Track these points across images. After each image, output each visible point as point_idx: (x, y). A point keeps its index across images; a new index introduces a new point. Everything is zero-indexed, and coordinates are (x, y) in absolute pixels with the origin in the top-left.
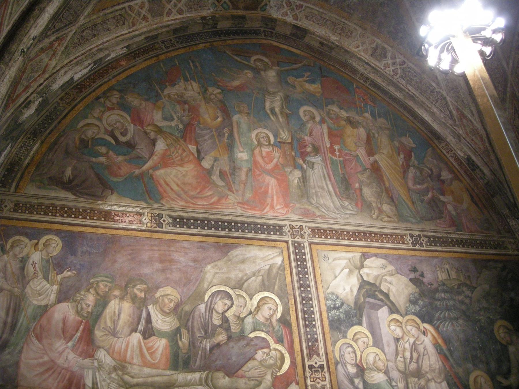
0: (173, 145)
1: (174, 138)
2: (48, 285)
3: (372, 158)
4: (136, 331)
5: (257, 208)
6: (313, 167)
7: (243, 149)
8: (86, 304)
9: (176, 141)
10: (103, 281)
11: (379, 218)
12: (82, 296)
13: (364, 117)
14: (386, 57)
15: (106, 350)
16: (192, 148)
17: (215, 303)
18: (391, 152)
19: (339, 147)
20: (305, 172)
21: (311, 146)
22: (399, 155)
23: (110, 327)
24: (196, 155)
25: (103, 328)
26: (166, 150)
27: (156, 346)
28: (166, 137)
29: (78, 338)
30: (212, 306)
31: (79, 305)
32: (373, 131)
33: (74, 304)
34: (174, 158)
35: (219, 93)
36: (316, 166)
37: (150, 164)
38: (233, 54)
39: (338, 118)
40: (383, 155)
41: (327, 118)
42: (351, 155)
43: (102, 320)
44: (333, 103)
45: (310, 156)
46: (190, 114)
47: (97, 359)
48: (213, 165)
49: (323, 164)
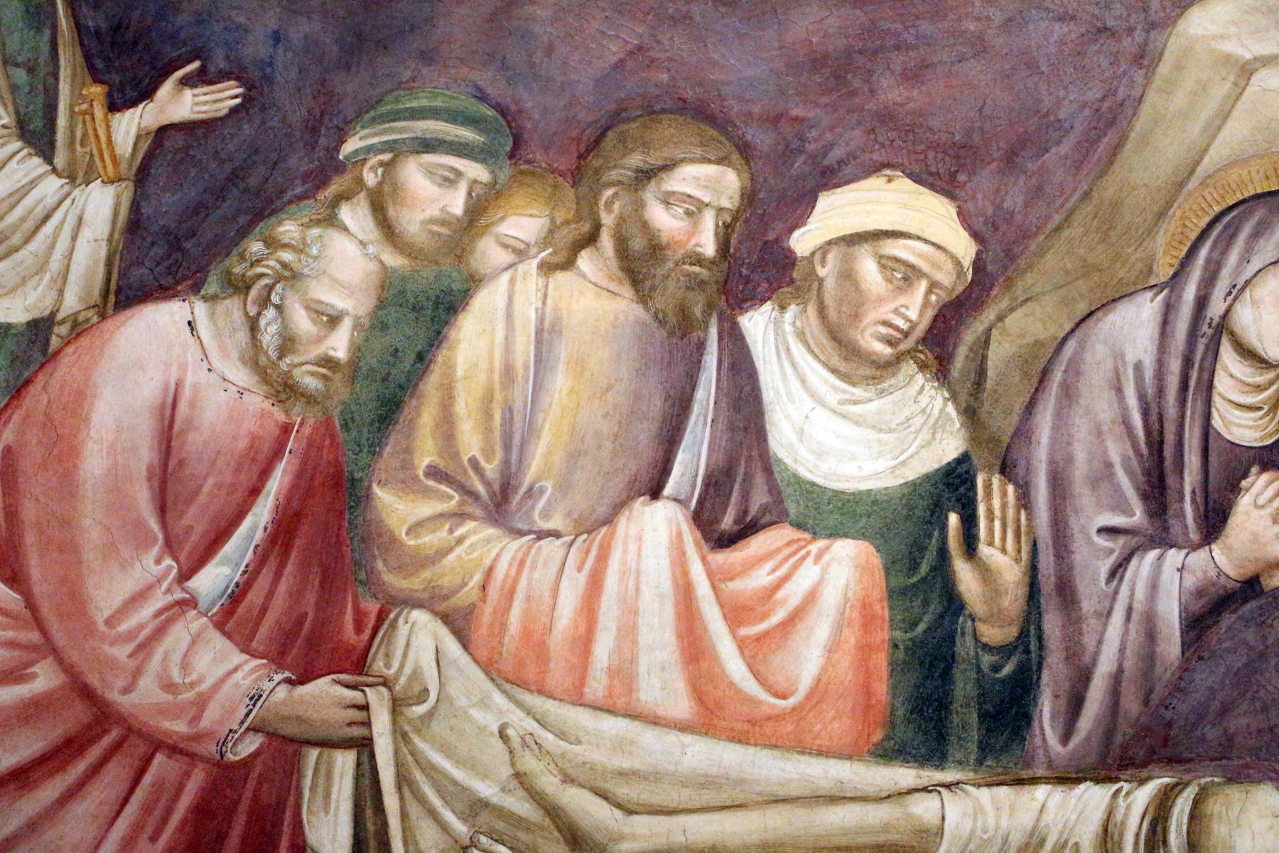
2: (52, 186)
4: (655, 493)
8: (316, 310)
10: (428, 145)
12: (287, 256)
15: (446, 618)
17: (1236, 292)
23: (474, 463)
25: (434, 473)
27: (794, 592)
29: (259, 535)
30: (1216, 308)
31: (270, 313)
33: (232, 308)
43: (426, 416)
47: (385, 683)
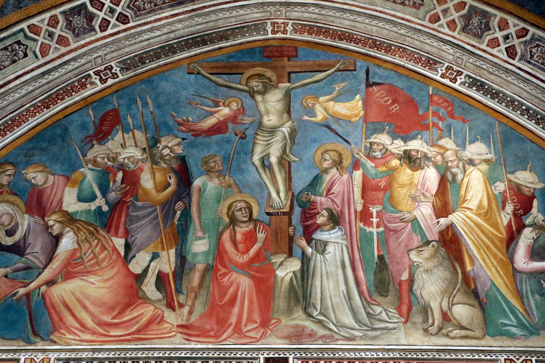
0: (88, 241)
1: (91, 229)
3: (443, 221)
5: (212, 333)
6: (324, 250)
7: (204, 233)
9: (93, 234)
11: (444, 331)
13: (441, 147)
14: (489, 29)
16: (119, 243)
18: (485, 203)
19: (379, 208)
20: (309, 260)
21: (325, 213)
22: (503, 208)
24: (122, 254)
26: (75, 250)
28: (78, 228)
32: (454, 170)
34: (86, 260)
35: (178, 144)
36: (330, 248)
37: (46, 275)
38: (212, 74)
39: (387, 153)
40: (468, 213)
41: (364, 159)
42: (402, 220)
44: (382, 131)
45: (322, 231)
46: (124, 185)
48: (148, 266)
49: (345, 242)
